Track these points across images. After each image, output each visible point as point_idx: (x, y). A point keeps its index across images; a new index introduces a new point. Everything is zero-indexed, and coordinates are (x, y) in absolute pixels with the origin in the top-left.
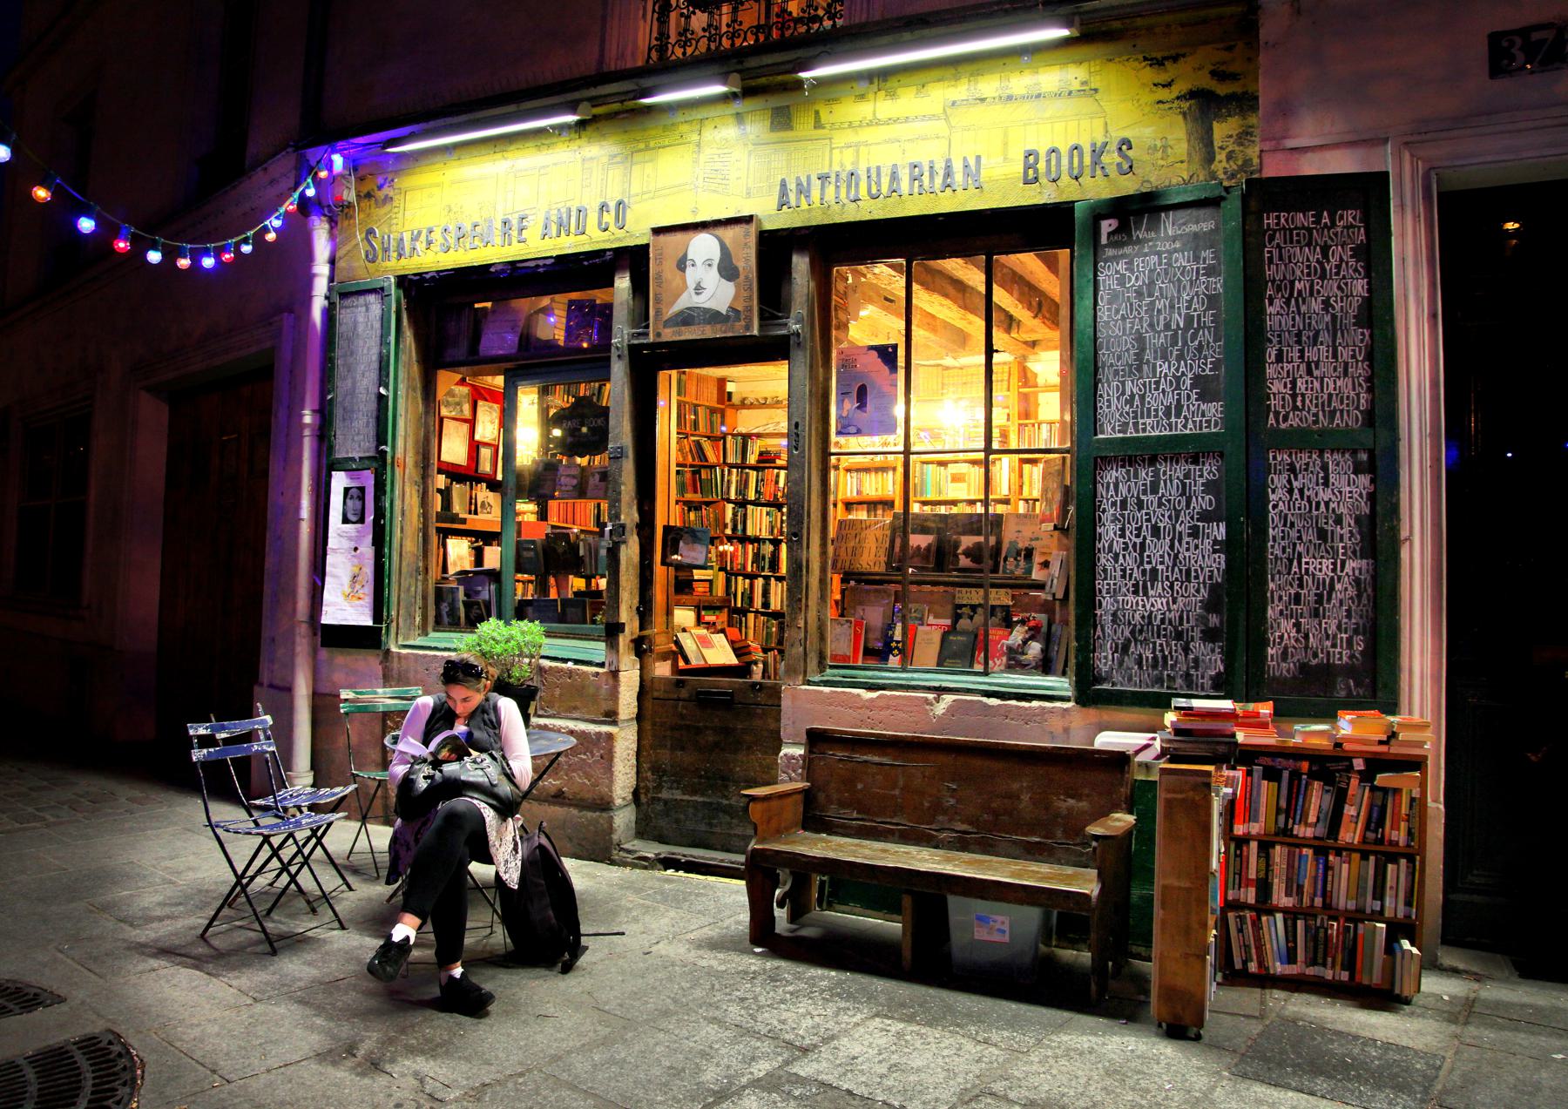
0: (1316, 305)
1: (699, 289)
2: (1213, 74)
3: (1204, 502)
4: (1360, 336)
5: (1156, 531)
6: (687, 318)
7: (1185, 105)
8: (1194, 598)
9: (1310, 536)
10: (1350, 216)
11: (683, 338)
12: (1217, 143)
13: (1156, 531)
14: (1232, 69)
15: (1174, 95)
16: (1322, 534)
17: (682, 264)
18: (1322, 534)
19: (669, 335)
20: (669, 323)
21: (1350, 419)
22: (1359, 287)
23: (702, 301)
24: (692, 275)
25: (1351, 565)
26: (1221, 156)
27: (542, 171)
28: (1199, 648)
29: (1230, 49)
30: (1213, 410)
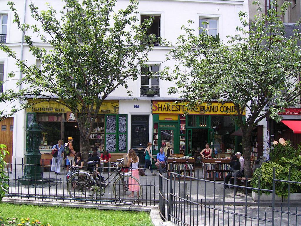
0: (122, 124)
1: (72, 118)
3: (114, 138)
4: (125, 126)
5: (111, 140)
6: (70, 120)
8: (113, 145)
9: (122, 140)
10: (125, 117)
13: (111, 140)
16: (122, 140)
17: (70, 115)
18: (122, 140)
19: (69, 122)
20: (69, 120)
21: (125, 132)
22: (125, 122)
23: (72, 119)
24: (71, 116)
25: (125, 142)
28: (114, 148)
30: (115, 131)
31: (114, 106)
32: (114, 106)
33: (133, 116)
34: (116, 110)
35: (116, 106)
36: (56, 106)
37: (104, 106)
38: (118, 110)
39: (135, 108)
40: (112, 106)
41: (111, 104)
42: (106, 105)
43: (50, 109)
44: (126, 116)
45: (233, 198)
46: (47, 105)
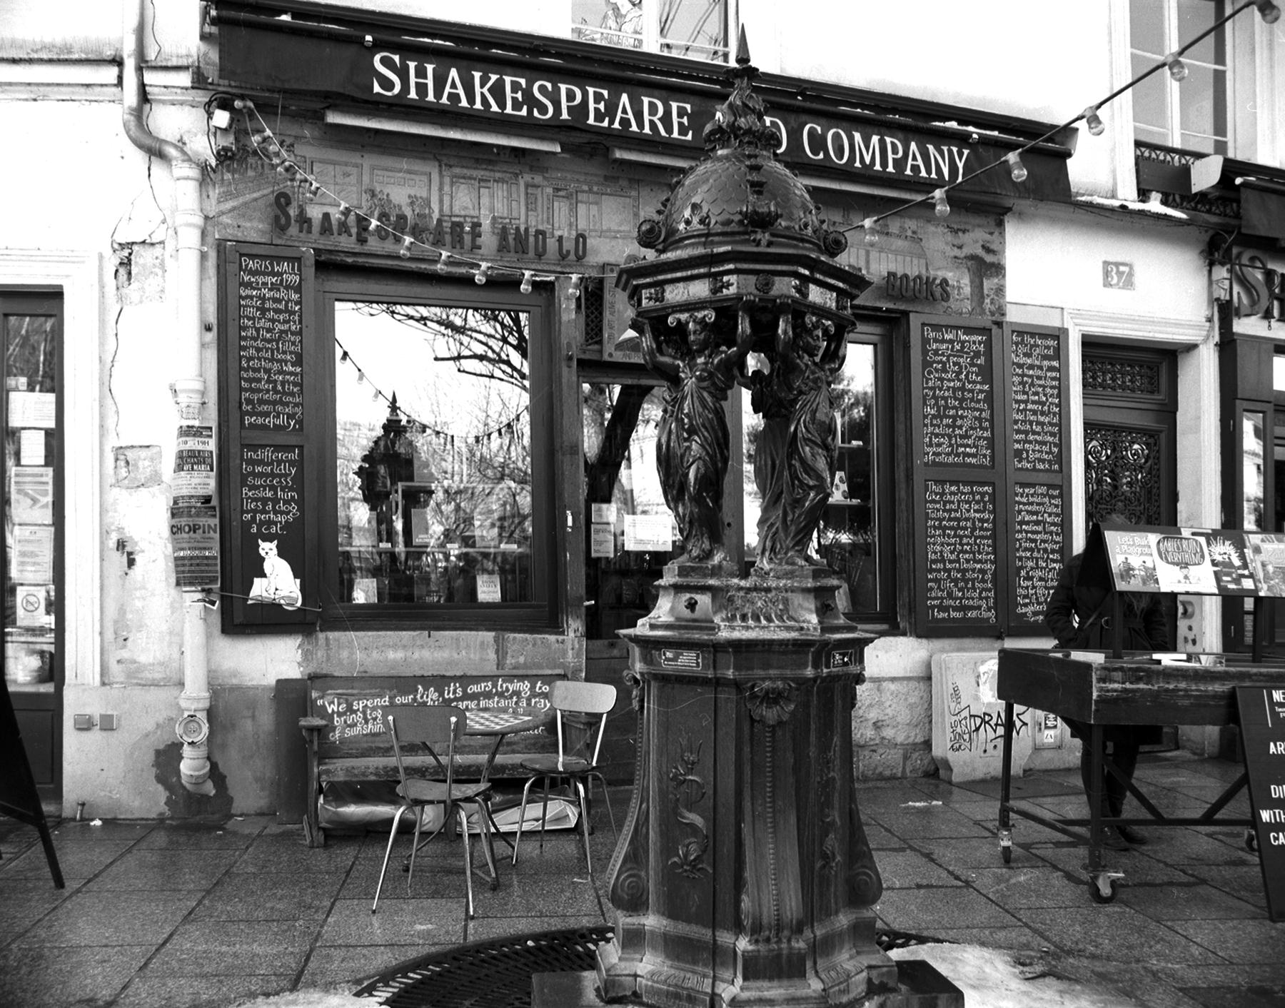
2: (983, 247)
7: (969, 263)
11: (632, 361)
12: (986, 292)
14: (993, 247)
15: (963, 255)
19: (619, 357)
26: (988, 301)
27: (482, 184)
29: (991, 234)
31: (967, 251)
32: (973, 258)
33: (1089, 344)
34: (988, 284)
35: (989, 258)
36: (501, 209)
37: (900, 243)
38: (1000, 290)
39: (1107, 284)
40: (957, 252)
41: (949, 237)
42: (916, 239)
43: (457, 226)
44: (1058, 336)
45: (1081, 793)
46: (424, 195)
